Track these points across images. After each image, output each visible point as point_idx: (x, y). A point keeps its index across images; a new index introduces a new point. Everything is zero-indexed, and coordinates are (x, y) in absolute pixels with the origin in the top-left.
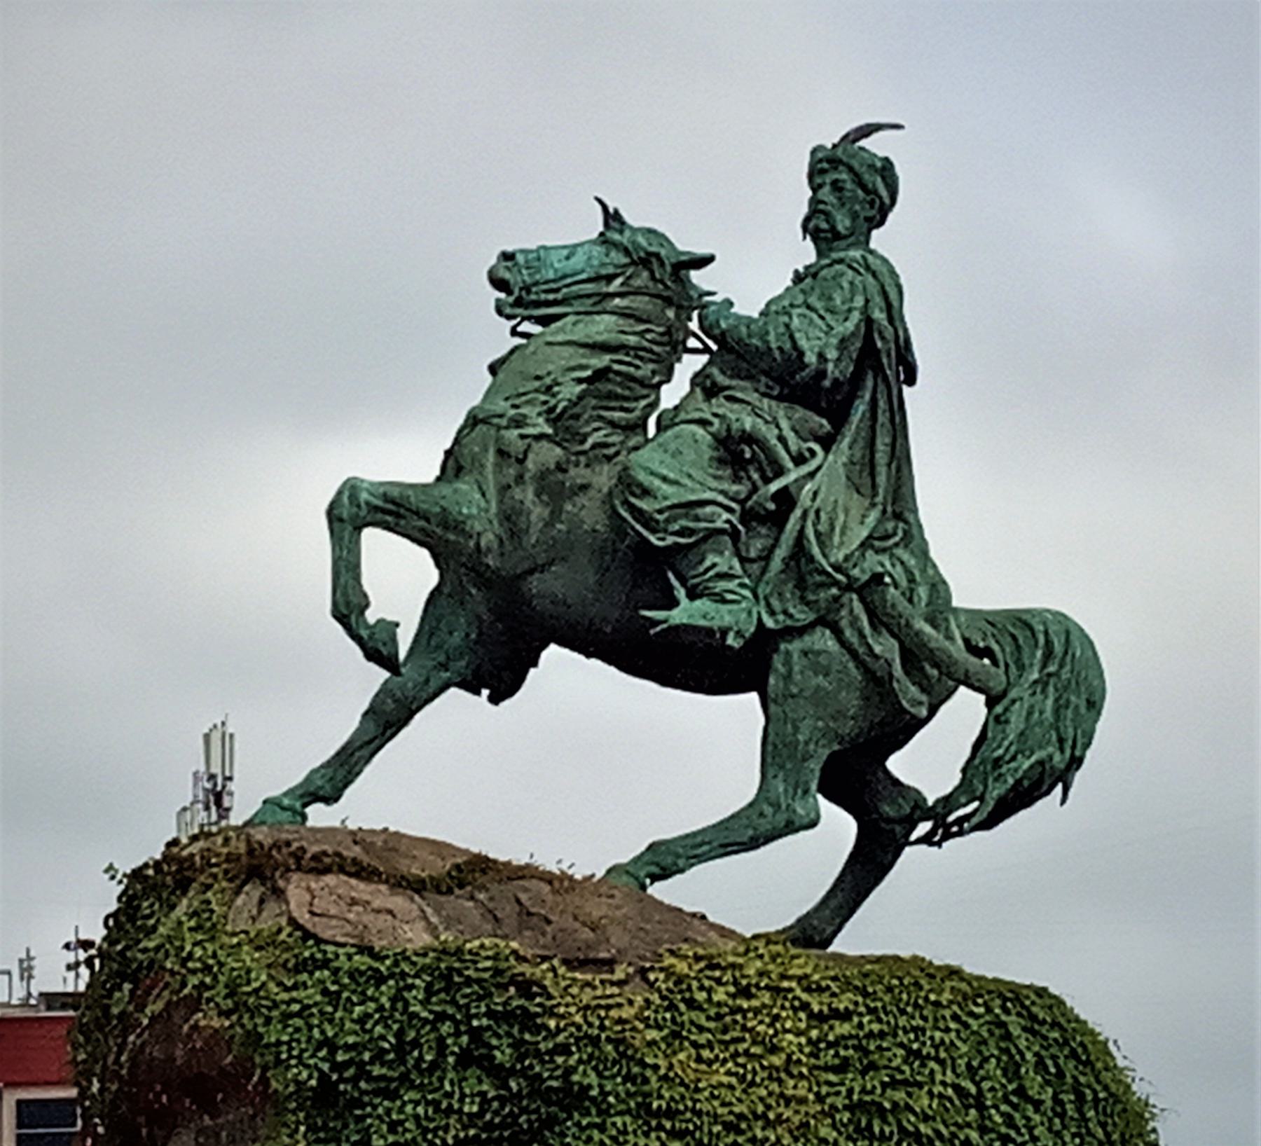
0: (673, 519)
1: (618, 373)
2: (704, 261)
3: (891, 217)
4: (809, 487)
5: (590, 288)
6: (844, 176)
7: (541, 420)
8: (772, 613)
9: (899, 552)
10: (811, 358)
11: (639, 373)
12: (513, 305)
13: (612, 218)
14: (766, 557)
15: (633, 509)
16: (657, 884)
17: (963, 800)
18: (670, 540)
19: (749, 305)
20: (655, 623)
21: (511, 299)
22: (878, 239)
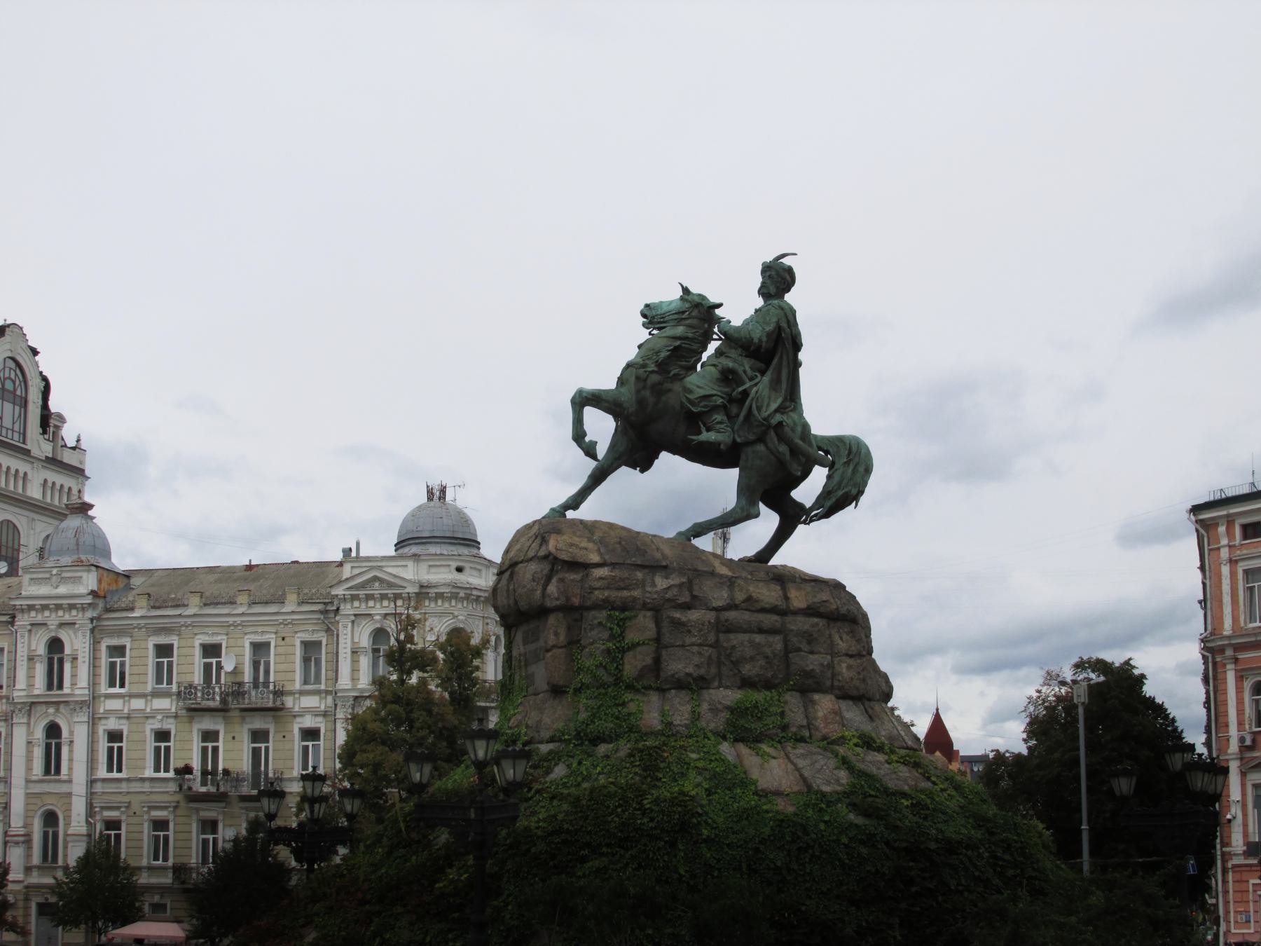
0: (700, 402)
1: (684, 348)
2: (719, 305)
3: (793, 289)
4: (755, 389)
5: (676, 316)
7: (653, 365)
8: (740, 436)
9: (791, 414)
10: (756, 340)
11: (693, 347)
12: (650, 323)
13: (686, 290)
14: (738, 415)
15: (687, 397)
16: (696, 539)
17: (817, 507)
18: (699, 409)
19: (737, 321)
20: (693, 440)
22: (788, 297)
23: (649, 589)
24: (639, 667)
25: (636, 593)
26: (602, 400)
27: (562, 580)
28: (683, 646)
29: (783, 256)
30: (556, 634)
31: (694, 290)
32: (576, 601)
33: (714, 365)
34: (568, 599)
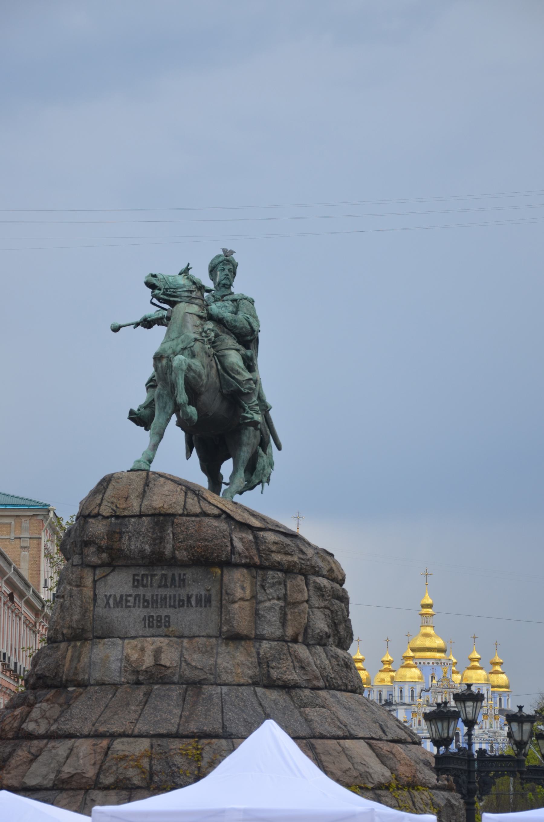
0: (246, 384)
5: (186, 294)
6: (232, 267)
12: (162, 294)
15: (233, 378)
18: (247, 391)
20: (247, 418)
21: (162, 292)
23: (302, 556)
24: (302, 624)
25: (296, 559)
26: (192, 369)
27: (241, 539)
28: (318, 608)
29: (232, 252)
30: (243, 588)
31: (190, 272)
32: (257, 560)
33: (238, 350)
34: (251, 558)
